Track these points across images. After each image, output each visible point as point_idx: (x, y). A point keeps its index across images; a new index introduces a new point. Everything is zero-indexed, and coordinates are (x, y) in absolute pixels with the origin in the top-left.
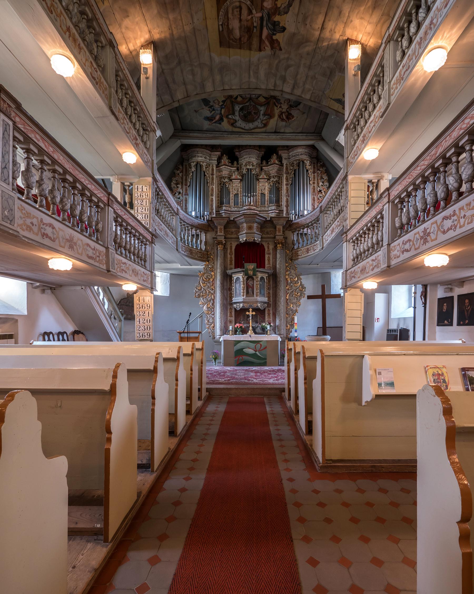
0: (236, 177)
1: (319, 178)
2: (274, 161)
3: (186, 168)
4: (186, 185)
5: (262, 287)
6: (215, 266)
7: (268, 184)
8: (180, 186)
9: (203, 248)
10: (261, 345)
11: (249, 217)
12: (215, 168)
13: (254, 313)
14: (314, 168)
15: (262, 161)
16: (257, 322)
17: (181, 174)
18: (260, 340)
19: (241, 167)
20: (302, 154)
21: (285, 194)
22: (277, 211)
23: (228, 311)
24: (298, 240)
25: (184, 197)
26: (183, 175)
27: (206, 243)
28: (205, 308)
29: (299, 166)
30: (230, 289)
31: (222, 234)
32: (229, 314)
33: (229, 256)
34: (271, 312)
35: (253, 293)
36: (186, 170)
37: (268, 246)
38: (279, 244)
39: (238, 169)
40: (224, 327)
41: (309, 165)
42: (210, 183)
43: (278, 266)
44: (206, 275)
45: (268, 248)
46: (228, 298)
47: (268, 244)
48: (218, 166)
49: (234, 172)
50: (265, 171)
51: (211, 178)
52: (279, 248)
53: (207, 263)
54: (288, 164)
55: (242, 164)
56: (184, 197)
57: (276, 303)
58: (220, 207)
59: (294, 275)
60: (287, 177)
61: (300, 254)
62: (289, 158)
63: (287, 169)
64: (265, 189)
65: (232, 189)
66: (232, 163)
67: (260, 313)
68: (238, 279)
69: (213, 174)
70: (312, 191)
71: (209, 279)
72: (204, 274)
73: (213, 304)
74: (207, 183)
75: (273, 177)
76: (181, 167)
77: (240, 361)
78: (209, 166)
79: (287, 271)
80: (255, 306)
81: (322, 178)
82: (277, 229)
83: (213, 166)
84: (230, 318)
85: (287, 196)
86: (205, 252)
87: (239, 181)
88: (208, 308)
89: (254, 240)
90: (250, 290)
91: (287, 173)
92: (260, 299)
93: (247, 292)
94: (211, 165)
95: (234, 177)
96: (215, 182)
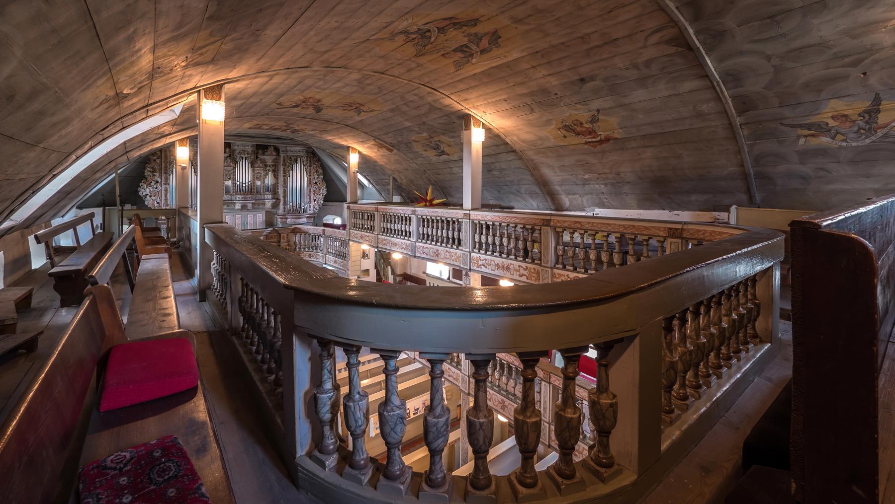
4: (166, 173)
8: (157, 174)
15: (257, 149)
19: (234, 154)
25: (163, 186)
56: (163, 186)
63: (284, 160)
91: (284, 165)
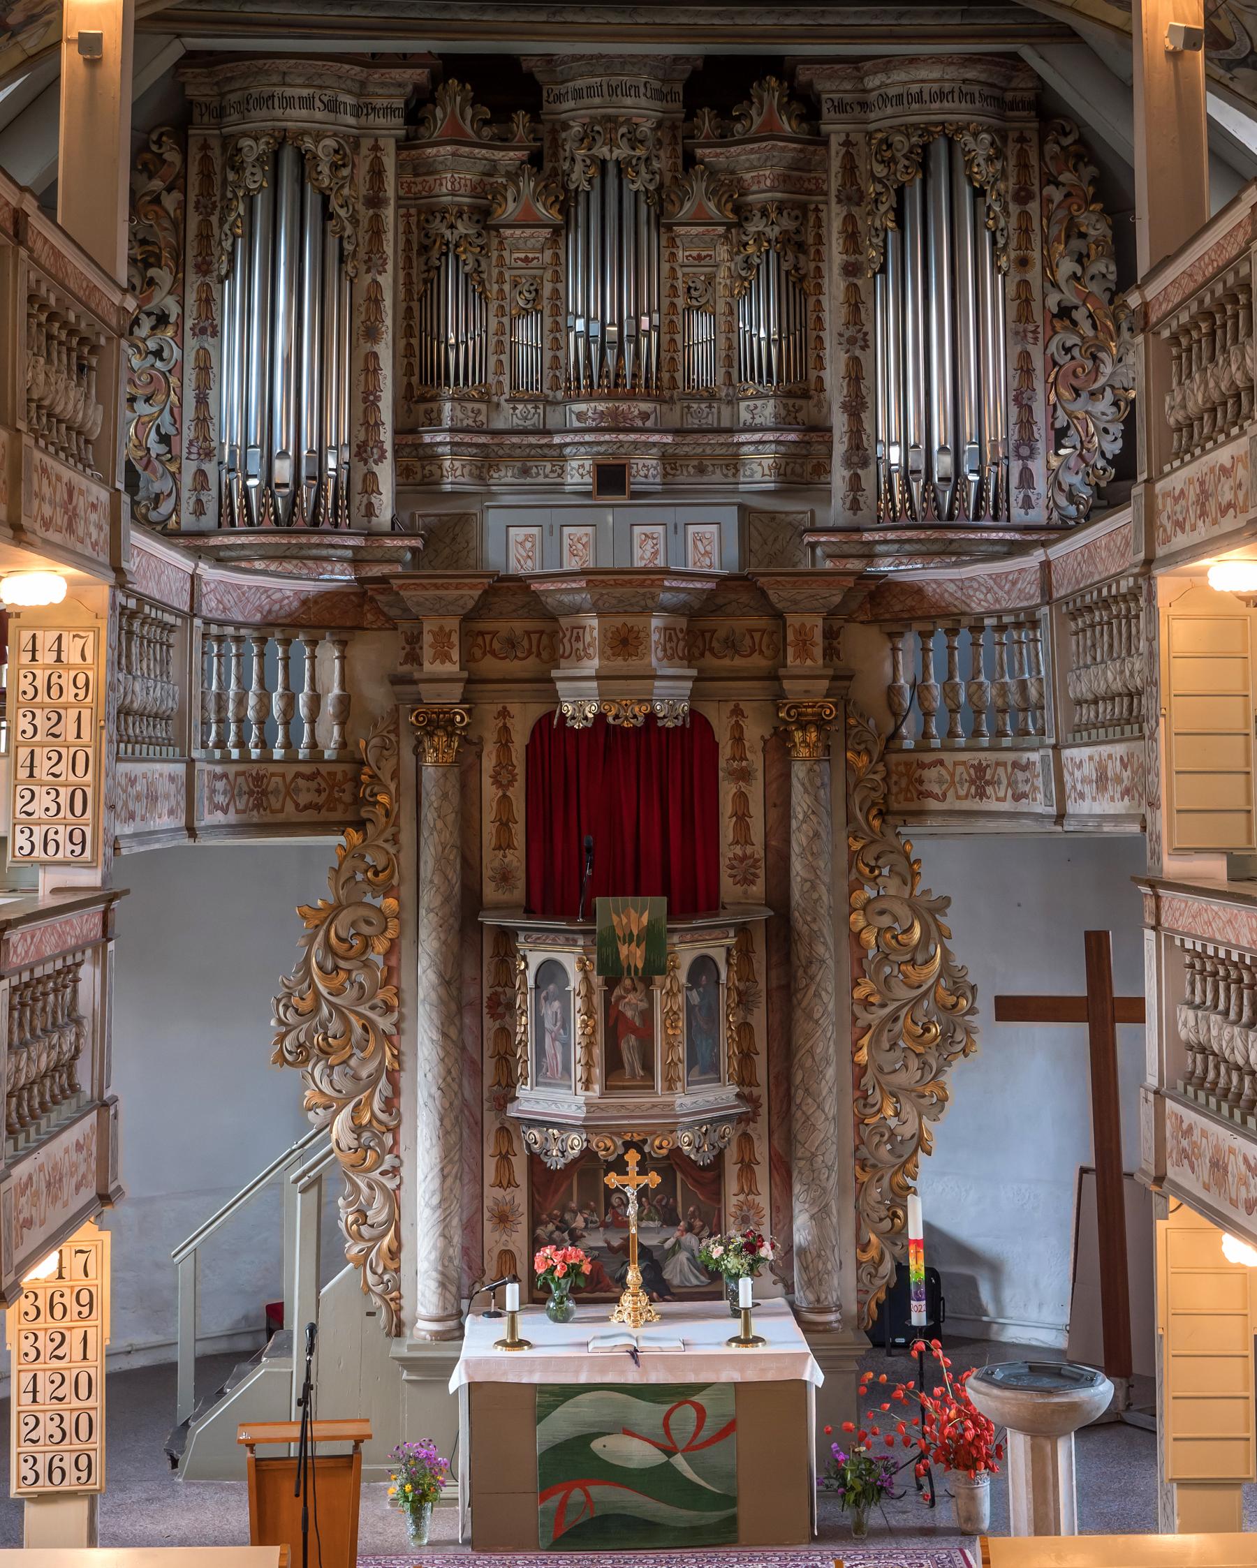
3: (206, 160)
4: (204, 268)
5: (701, 1023)
6: (406, 858)
8: (163, 275)
9: (330, 736)
10: (700, 1410)
11: (617, 584)
12: (389, 163)
13: (653, 1179)
16: (670, 1220)
18: (691, 1378)
19: (556, 145)
20: (942, 96)
22: (792, 437)
23: (489, 1149)
24: (919, 688)
25: (191, 343)
26: (183, 206)
27: (345, 702)
28: (341, 1124)
29: (924, 167)
30: (503, 1007)
31: (452, 668)
32: (490, 1165)
33: (490, 792)
34: (762, 1151)
35: (648, 1067)
37: (738, 728)
38: (803, 727)
39: (536, 160)
40: (465, 1251)
41: (989, 159)
42: (362, 255)
43: (797, 866)
44: (346, 917)
45: (738, 739)
46: (489, 1066)
47: (737, 712)
48: (403, 145)
49: (513, 177)
50: (712, 172)
51: (364, 223)
52: (804, 752)
53: (356, 837)
55: (566, 126)
56: (191, 343)
57: (788, 1098)
58: (423, 399)
59: (903, 911)
60: (849, 219)
61: (936, 789)
62: (864, 105)
63: (850, 168)
64: (710, 280)
66: (501, 115)
67: (690, 1187)
68: (550, 971)
69: (375, 201)
70: (1012, 314)
71: (367, 944)
72: (337, 909)
73: (390, 1105)
74: (342, 260)
75: (764, 213)
76: (173, 157)
77: (571, 1519)
78: (356, 146)
79: (856, 886)
80: (659, 1146)
81: (1073, 231)
82: (790, 637)
83: (376, 148)
84: (499, 1193)
86: (339, 768)
87: (546, 233)
88: (358, 1129)
89: (651, 717)
90: (629, 1047)
91: (852, 196)
92: (691, 1104)
93: (613, 1064)
94: (366, 144)
95: (509, 209)
96: (389, 249)
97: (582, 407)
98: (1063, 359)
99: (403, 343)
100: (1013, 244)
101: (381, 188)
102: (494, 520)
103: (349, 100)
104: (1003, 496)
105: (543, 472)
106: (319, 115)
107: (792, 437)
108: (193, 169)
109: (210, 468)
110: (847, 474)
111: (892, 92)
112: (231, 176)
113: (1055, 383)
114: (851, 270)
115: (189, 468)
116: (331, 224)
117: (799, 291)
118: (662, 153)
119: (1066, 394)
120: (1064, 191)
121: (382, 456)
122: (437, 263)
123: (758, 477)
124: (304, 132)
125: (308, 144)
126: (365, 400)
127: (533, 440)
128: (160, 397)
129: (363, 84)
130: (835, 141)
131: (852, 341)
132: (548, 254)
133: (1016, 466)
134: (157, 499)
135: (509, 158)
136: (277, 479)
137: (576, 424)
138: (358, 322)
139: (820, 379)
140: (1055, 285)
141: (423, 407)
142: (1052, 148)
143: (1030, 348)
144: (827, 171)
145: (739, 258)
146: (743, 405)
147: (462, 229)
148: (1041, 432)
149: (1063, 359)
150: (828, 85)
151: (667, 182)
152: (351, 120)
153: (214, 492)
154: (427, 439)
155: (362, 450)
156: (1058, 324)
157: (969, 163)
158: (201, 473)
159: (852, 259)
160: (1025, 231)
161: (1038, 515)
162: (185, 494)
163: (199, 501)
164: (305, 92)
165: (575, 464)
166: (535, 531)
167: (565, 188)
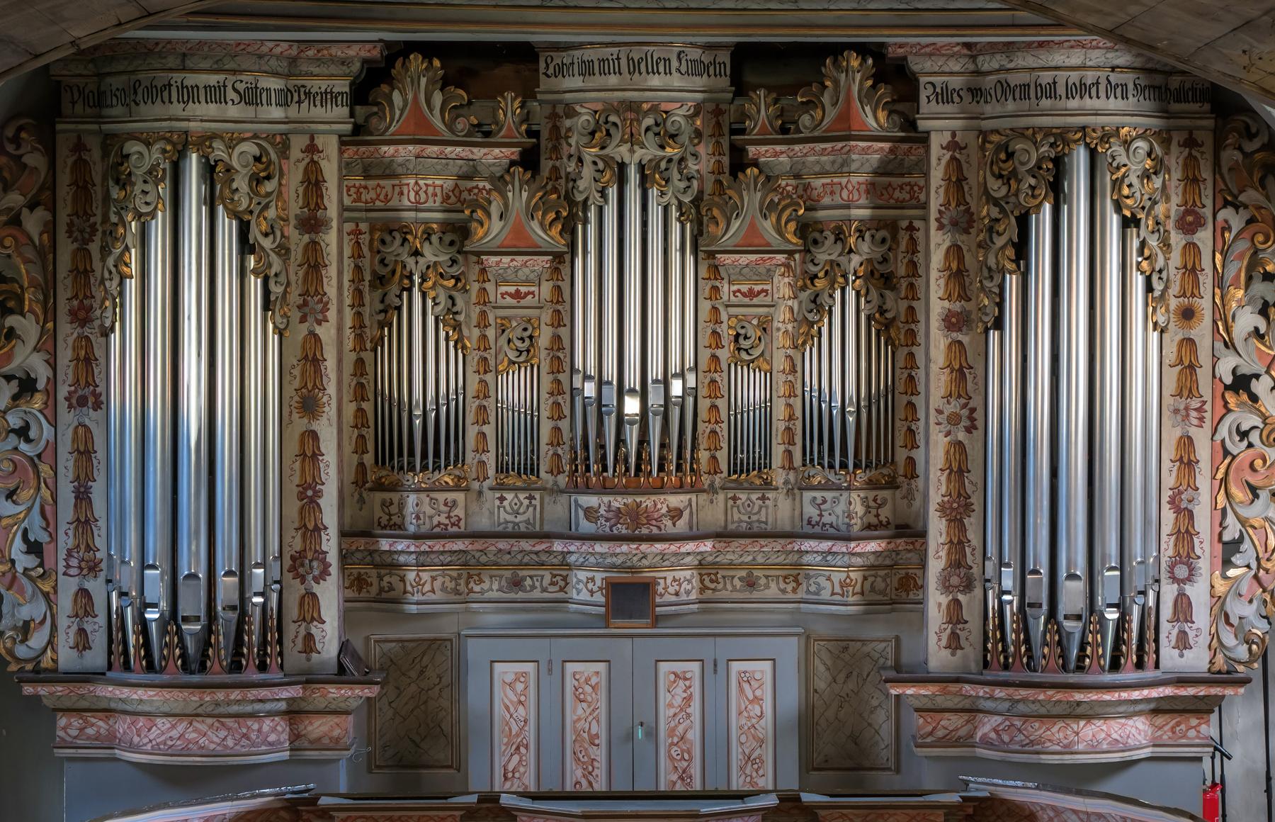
0: (519, 231)
1: (1237, 268)
2: (845, 117)
3: (81, 166)
4: (82, 316)
7: (797, 290)
14: (1191, 181)
17: (33, 223)
19: (558, 136)
20: (1083, 89)
21: (936, 399)
25: (67, 418)
26: (51, 228)
36: (83, 188)
39: (529, 161)
41: (1146, 176)
42: (295, 298)
49: (500, 182)
51: (297, 254)
54: (973, 141)
55: (571, 113)
56: (67, 418)
58: (379, 486)
60: (955, 251)
63: (957, 182)
64: (765, 326)
65: (483, 323)
69: (312, 223)
74: (267, 305)
75: (839, 237)
76: (35, 160)
78: (284, 149)
83: (312, 149)
85: (954, 420)
87: (543, 262)
91: (962, 222)
94: (298, 144)
95: (492, 230)
96: (331, 290)
97: (591, 501)
98: (1236, 447)
99: (350, 409)
100: (1175, 289)
101: (319, 206)
102: (476, 651)
103: (275, 84)
104: (1150, 635)
105: (539, 584)
106: (233, 111)
107: (873, 546)
108: (64, 178)
109: (96, 586)
110: (944, 600)
111: (1014, 79)
112: (116, 193)
113: (1225, 481)
114: (953, 322)
115: (68, 588)
116: (252, 261)
117: (892, 329)
118: (702, 150)
119: (1239, 494)
120: (1244, 215)
121: (325, 573)
122: (396, 302)
123: (826, 595)
124: (213, 136)
125: (219, 151)
126: (301, 496)
127: (525, 545)
128: (25, 494)
129: (293, 61)
130: (936, 142)
131: (954, 420)
132: (546, 288)
133: (1169, 592)
134: (25, 630)
135: (494, 157)
136: (185, 609)
137: (586, 526)
138: (289, 391)
139: (911, 462)
140: (1229, 345)
141: (379, 496)
142: (1231, 156)
143: (1193, 432)
144: (926, 175)
145: (805, 295)
146: (808, 495)
147: (430, 254)
148: (1205, 547)
149: (1236, 447)
150: (928, 65)
151: (709, 188)
152: (277, 113)
153: (102, 620)
154: (384, 544)
155: (301, 563)
156: (1231, 399)
157: (1117, 184)
158: (84, 593)
159: (957, 306)
160: (1191, 271)
161: (1197, 660)
162: (63, 622)
163: (82, 631)
164: (213, 79)
165: (582, 575)
166: (530, 668)
167: (569, 198)
